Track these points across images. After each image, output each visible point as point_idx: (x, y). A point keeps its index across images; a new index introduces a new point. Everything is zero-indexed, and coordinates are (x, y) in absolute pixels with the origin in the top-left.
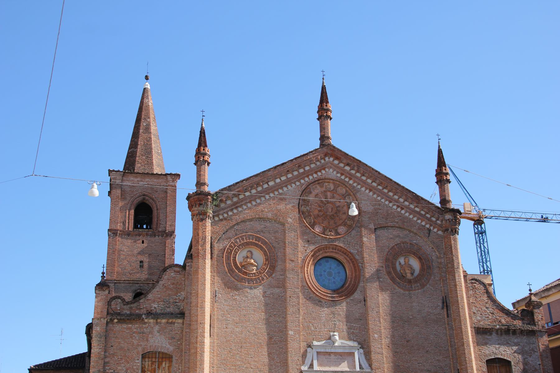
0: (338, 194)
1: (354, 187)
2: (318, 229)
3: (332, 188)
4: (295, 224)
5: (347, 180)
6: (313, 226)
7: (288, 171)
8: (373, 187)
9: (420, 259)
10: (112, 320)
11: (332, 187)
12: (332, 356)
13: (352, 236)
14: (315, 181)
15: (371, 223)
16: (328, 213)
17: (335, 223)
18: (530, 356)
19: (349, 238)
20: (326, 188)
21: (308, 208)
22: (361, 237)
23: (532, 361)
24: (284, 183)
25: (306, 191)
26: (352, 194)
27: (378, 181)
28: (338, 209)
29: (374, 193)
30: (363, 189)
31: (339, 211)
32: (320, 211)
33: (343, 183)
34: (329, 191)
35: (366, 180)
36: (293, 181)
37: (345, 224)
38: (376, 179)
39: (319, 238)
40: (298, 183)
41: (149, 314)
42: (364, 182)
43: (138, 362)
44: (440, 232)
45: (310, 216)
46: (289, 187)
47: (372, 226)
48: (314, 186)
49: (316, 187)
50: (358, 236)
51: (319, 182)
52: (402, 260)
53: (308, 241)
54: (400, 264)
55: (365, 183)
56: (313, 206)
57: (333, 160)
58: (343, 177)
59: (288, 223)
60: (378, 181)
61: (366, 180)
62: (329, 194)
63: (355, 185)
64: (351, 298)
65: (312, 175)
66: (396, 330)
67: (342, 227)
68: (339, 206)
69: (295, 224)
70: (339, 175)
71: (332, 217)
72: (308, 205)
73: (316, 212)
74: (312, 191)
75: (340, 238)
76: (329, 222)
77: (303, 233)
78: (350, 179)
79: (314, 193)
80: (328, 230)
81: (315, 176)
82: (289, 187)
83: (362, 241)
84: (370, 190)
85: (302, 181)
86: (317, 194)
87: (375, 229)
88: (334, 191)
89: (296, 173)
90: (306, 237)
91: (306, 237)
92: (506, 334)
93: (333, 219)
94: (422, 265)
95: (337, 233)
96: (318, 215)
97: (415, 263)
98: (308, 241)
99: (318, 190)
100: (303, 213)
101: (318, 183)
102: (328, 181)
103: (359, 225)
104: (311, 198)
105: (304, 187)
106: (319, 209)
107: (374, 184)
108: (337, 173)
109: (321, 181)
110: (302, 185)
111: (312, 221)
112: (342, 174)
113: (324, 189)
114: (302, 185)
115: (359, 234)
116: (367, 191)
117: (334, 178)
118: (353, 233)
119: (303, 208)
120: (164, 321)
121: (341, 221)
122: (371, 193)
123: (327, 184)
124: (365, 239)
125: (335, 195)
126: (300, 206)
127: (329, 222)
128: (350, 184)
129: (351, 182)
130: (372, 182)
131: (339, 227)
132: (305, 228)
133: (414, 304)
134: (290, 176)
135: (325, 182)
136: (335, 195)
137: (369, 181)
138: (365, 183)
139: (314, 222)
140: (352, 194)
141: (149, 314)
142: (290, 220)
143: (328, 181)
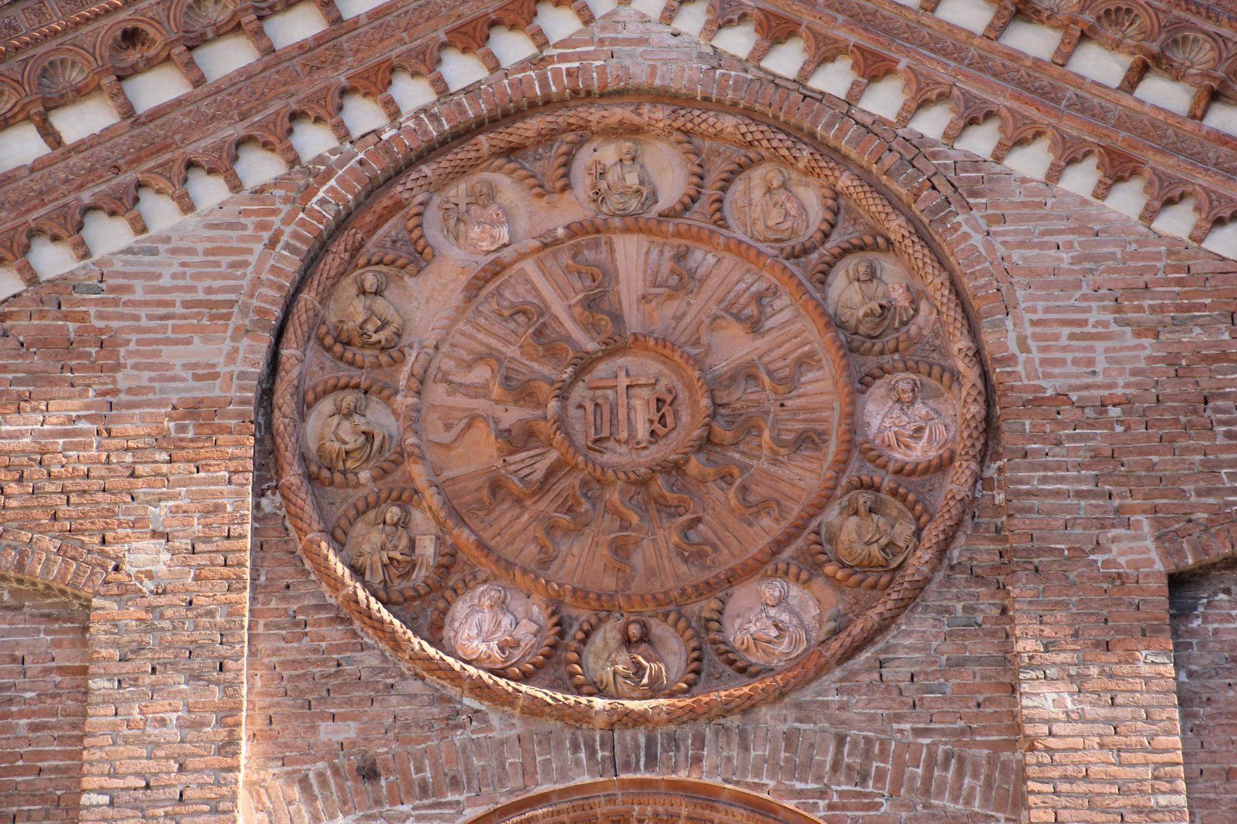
0: (738, 249)
1: (919, 148)
2: (483, 628)
3: (671, 183)
4: (212, 596)
5: (834, 79)
6: (427, 605)
7: (131, 37)
8: (1155, 129)
11: (669, 175)
13: (897, 673)
14: (463, 134)
15: (1122, 517)
16: (618, 455)
17: (695, 554)
19: (859, 707)
20: (598, 197)
21: (380, 418)
22: (1007, 677)
24: (92, 174)
25: (367, 227)
26: (896, 226)
27: (1201, 56)
28: (736, 396)
29: (1167, 197)
30: (1031, 162)
31: (748, 426)
32: (517, 440)
33: (785, 127)
34: (634, 224)
35: (1063, 57)
36: (197, 148)
37: (802, 551)
38: (1176, 35)
39: (501, 725)
42: (1043, 87)
45: (406, 497)
46: (160, 211)
47: (1139, 552)
48: (459, 191)
49: (489, 195)
50: (970, 676)
51: (510, 132)
53: (369, 773)
55: (1047, 96)
56: (438, 393)
58: (786, 61)
59: (125, 594)
60: (1201, 56)
61: (1063, 57)
62: (632, 258)
63: (932, 124)
65: (425, 63)
67: (772, 590)
68: (746, 373)
69: (212, 596)
70: (738, 41)
71: (661, 490)
72: (387, 393)
73: (478, 455)
74: (433, 231)
75: (747, 707)
76: (621, 550)
77: (308, 693)
78: (873, 69)
79: (456, 259)
80: (608, 634)
81: (461, 70)
82: (160, 211)
83: (1015, 729)
84: (1118, 169)
85: (314, 141)
86: (496, 269)
87: (1179, 582)
88: (697, 219)
89: (229, 58)
90: (348, 731)
91: (348, 731)
93: (672, 511)
95: (712, 657)
96: (496, 486)
98: (369, 773)
99: (503, 217)
100: (321, 473)
101: (511, 152)
102: (618, 113)
103: (986, 552)
104: (426, 305)
105: (326, 200)
106: (512, 416)
107: (1165, 95)
109: (532, 126)
110: (305, 177)
111: (427, 548)
113: (574, 208)
114: (305, 177)
115: (979, 648)
116: (1081, 180)
117: (681, 73)
118: (916, 638)
119: (325, 427)
121: (770, 527)
122: (1127, 200)
123: (609, 153)
124: (1044, 699)
125: (702, 259)
126: (284, 398)
127: (621, 550)
128: (871, 127)
129: (884, 101)
130: (1139, 72)
131: (743, 597)
132: (335, 634)
134: (157, 88)
135: (584, 134)
136: (702, 259)
137: (1100, 65)
138: (1047, 96)
139: (449, 561)
140: (896, 226)
142: (144, 557)
143: (618, 113)
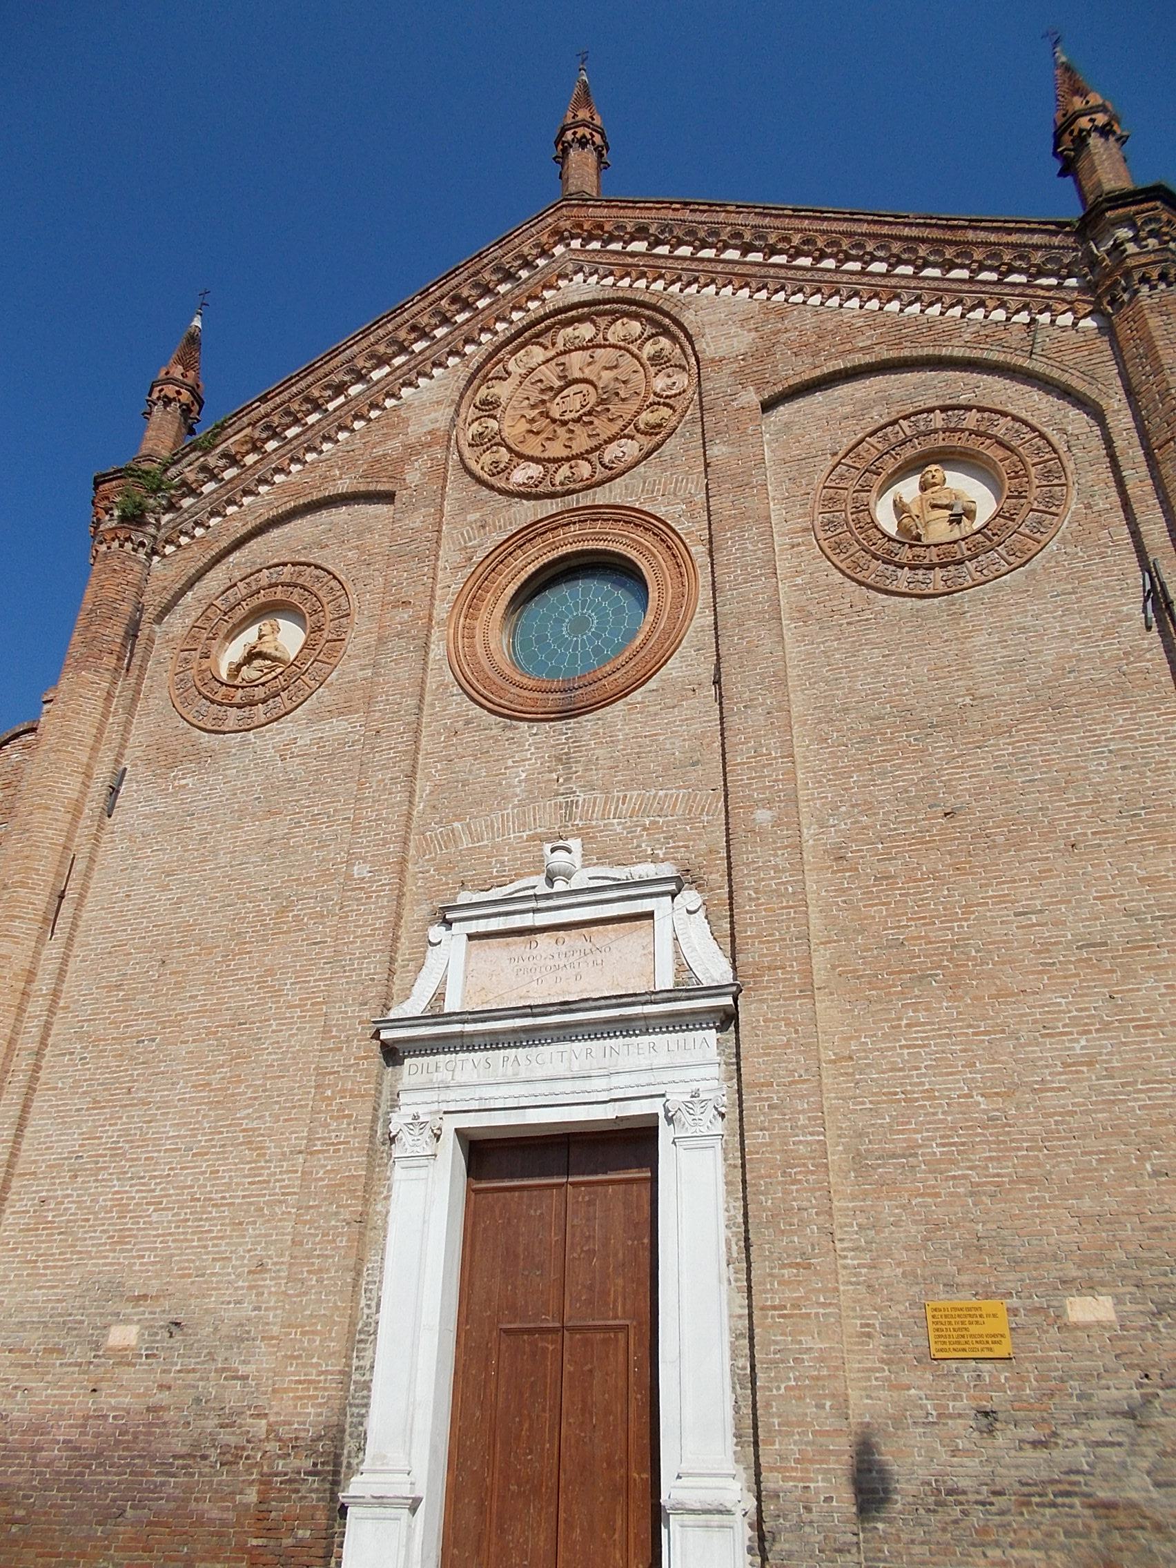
44: (1088, 323)
47: (751, 398)
52: (909, 489)
66: (883, 774)
105: (474, 364)
133: (981, 639)
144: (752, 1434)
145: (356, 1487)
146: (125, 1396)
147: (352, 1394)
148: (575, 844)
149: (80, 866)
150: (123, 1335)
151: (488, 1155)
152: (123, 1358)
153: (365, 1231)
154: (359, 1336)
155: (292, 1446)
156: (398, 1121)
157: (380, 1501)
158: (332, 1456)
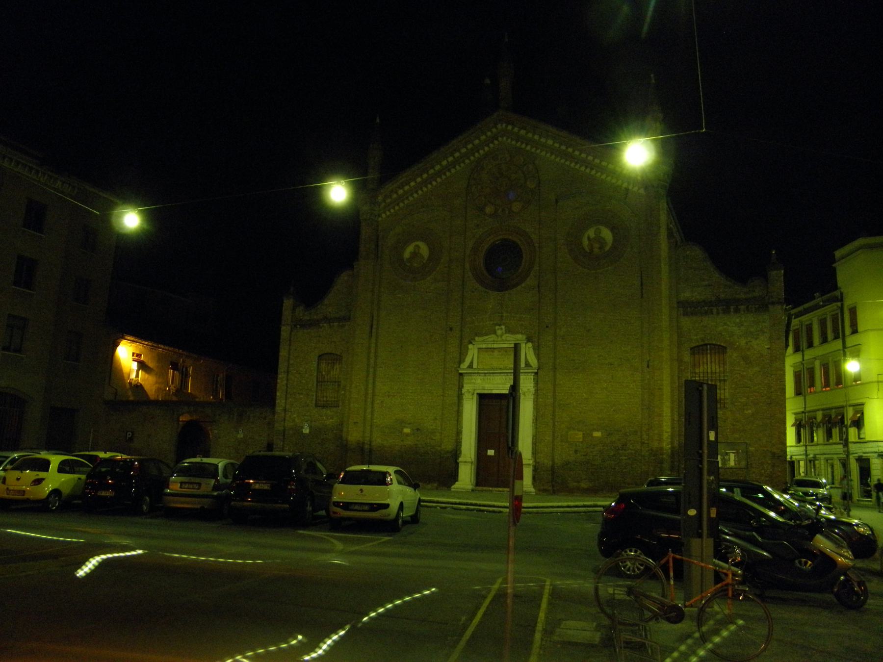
5: (523, 146)
9: (613, 229)
10: (295, 326)
12: (496, 353)
18: (756, 339)
23: (758, 345)
40: (467, 161)
41: (326, 319)
43: (315, 364)
52: (591, 233)
54: (589, 238)
57: (506, 126)
64: (523, 285)
82: (457, 167)
84: (552, 154)
87: (557, 201)
92: (724, 313)
94: (615, 235)
97: (607, 234)
108: (512, 140)
112: (517, 141)
120: (336, 324)
129: (528, 148)
141: (326, 319)
144: (535, 453)
145: (460, 459)
146: (409, 442)
147: (458, 443)
148: (503, 327)
149: (375, 318)
150: (407, 430)
151: (484, 399)
152: (407, 435)
153: (459, 413)
154: (459, 433)
155: (448, 452)
156: (464, 391)
157: (465, 462)
158: (456, 453)
